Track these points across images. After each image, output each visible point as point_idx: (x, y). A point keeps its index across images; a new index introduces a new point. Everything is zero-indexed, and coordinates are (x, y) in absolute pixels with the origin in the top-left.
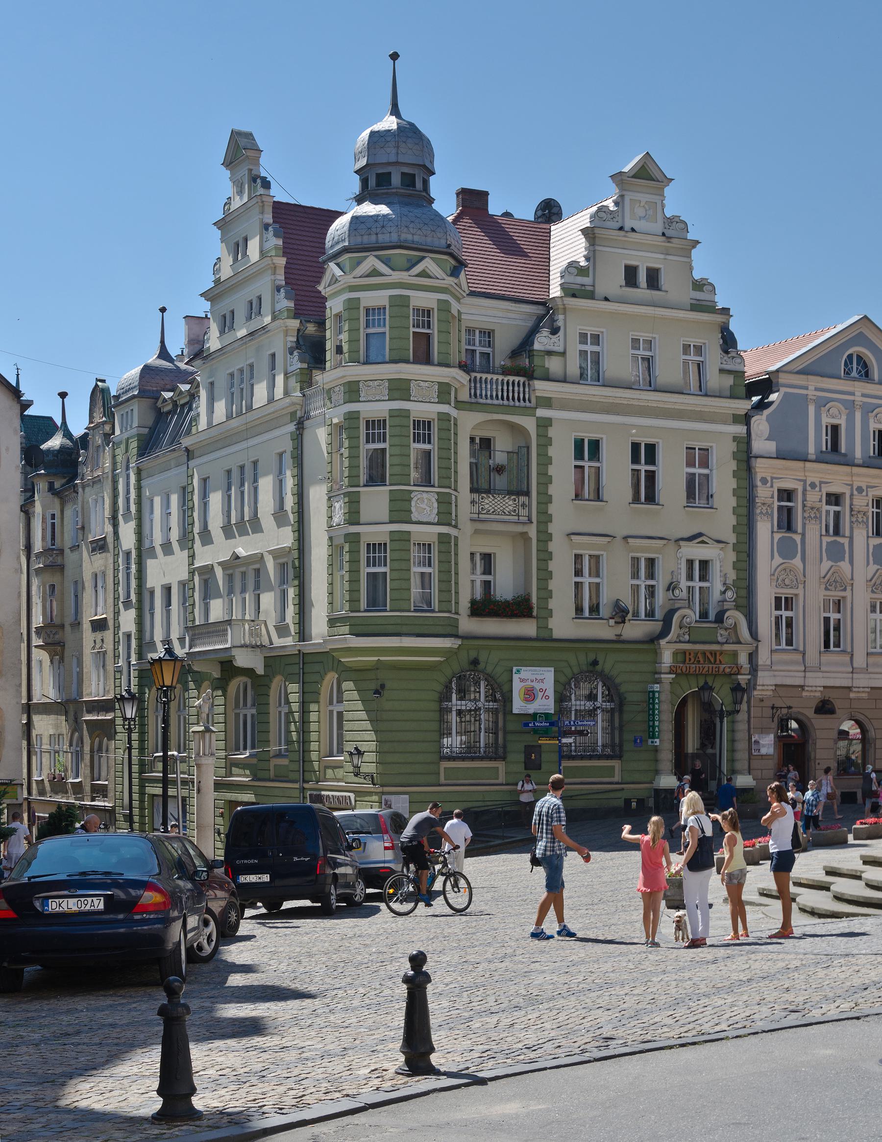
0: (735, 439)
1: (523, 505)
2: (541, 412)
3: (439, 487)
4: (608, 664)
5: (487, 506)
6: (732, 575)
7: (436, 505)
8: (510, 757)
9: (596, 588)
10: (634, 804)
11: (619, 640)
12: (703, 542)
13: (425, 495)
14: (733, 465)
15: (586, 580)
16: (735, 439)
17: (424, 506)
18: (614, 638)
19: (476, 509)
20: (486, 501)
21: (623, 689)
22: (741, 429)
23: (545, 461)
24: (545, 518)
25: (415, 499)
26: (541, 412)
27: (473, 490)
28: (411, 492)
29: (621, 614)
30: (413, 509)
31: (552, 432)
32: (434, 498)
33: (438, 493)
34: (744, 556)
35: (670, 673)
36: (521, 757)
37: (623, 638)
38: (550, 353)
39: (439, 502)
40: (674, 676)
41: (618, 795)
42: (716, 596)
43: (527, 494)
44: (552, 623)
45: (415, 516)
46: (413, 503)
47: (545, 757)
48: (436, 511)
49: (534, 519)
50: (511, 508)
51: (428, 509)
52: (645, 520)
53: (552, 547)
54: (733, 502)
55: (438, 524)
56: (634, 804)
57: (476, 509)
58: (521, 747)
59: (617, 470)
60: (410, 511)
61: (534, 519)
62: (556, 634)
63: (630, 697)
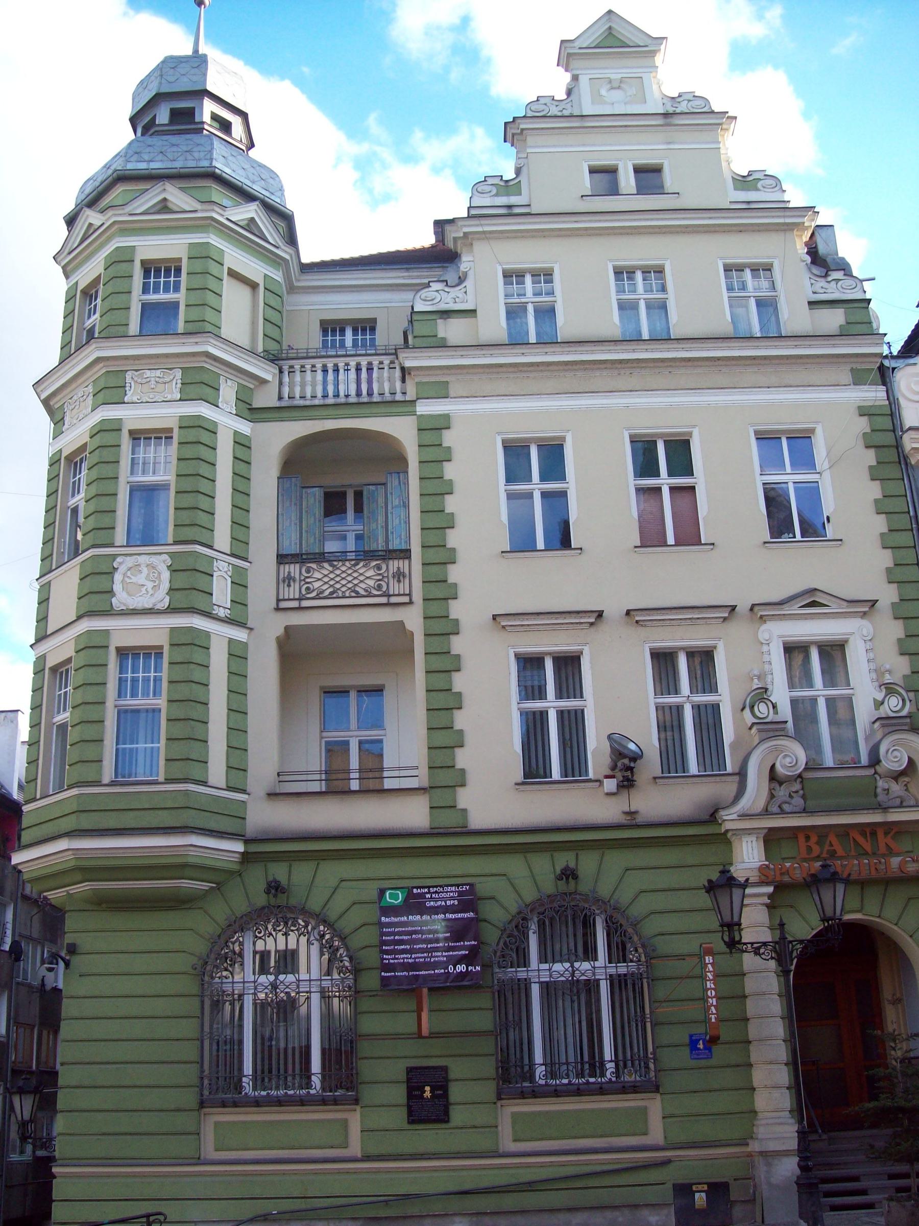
0: (864, 412)
1: (399, 576)
2: (424, 408)
3: (176, 543)
4: (604, 876)
5: (317, 585)
7: (166, 575)
8: (368, 1094)
9: (572, 723)
10: (700, 1199)
11: (632, 820)
12: (813, 604)
13: (142, 559)
14: (870, 458)
15: (551, 704)
16: (864, 412)
17: (141, 579)
18: (623, 819)
19: (293, 591)
20: (317, 575)
21: (650, 927)
22: (875, 395)
23: (437, 489)
24: (440, 592)
25: (122, 569)
26: (424, 408)
27: (282, 559)
28: (114, 557)
29: (625, 765)
30: (117, 587)
31: (448, 438)
32: (162, 563)
33: (172, 555)
35: (761, 883)
36: (399, 1094)
37: (639, 819)
38: (446, 314)
39: (173, 570)
40: (770, 889)
41: (654, 1175)
42: (864, 713)
43: (406, 554)
44: (464, 798)
45: (121, 598)
46: (118, 577)
47: (456, 1092)
48: (166, 586)
49: (417, 596)
50: (371, 583)
51: (150, 585)
52: (674, 577)
53: (458, 645)
54: (880, 524)
55: (172, 610)
56: (700, 1199)
57: (293, 591)
58: (398, 1070)
59: (600, 491)
60: (111, 592)
61: (417, 596)
62: (477, 821)
63: (664, 946)
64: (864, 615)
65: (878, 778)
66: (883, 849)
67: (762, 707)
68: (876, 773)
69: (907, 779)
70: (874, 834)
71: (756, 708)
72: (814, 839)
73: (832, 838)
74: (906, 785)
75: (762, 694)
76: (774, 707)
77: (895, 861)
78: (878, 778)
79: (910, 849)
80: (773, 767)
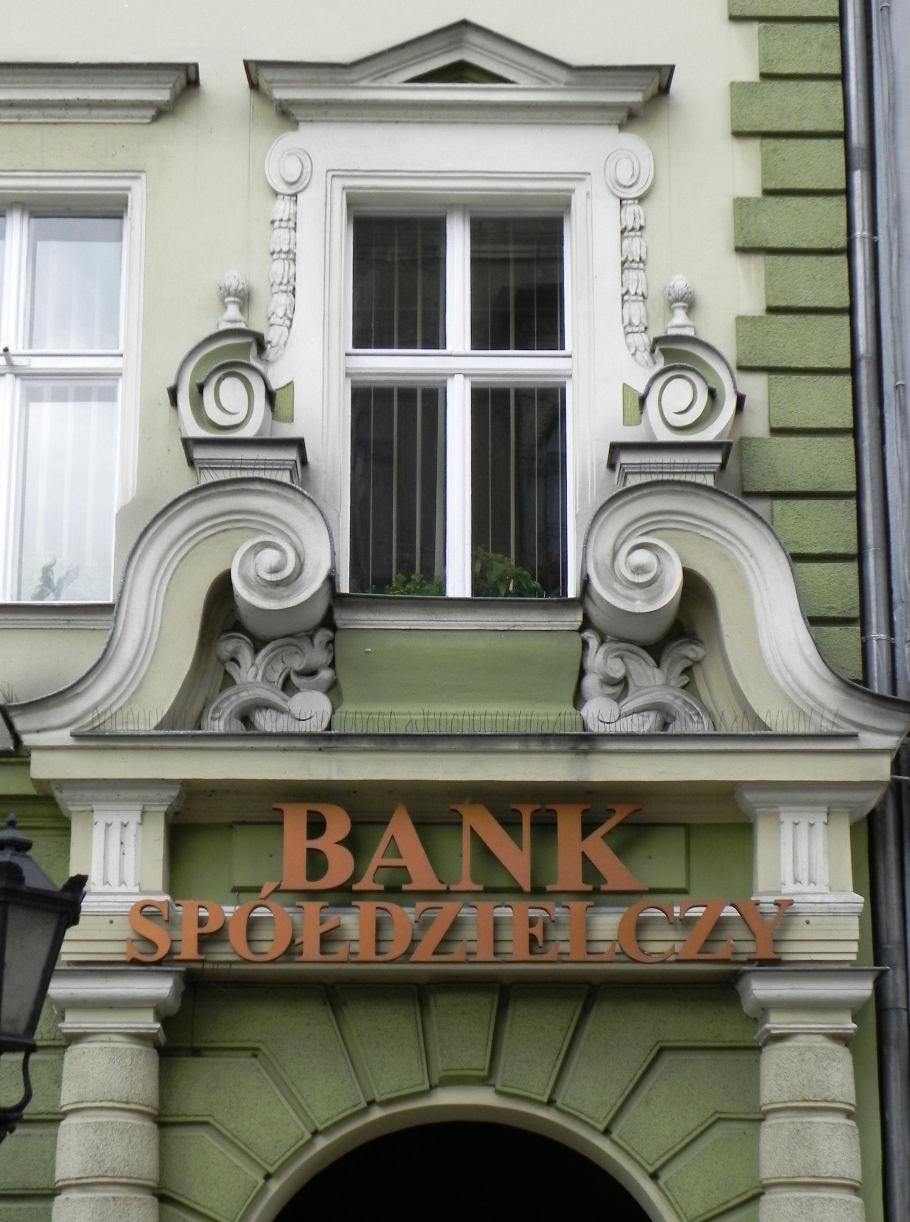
6: (730, 294)
34: (823, 163)
64: (630, 118)
65: (593, 642)
66: (567, 874)
67: (232, 392)
68: (587, 624)
69: (692, 651)
70: (545, 827)
71: (208, 395)
72: (339, 824)
73: (401, 829)
74: (687, 671)
75: (239, 350)
76: (271, 396)
77: (608, 923)
78: (593, 642)
79: (681, 884)
80: (222, 589)
